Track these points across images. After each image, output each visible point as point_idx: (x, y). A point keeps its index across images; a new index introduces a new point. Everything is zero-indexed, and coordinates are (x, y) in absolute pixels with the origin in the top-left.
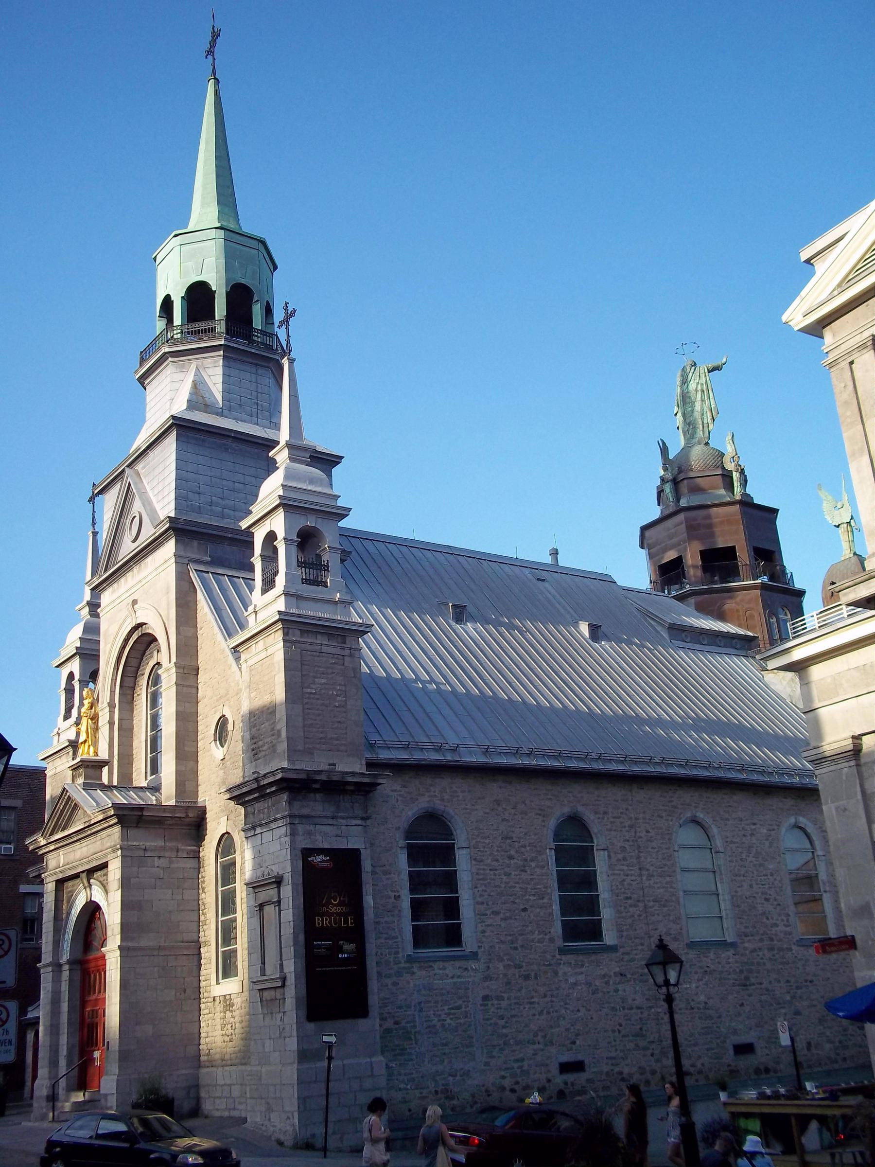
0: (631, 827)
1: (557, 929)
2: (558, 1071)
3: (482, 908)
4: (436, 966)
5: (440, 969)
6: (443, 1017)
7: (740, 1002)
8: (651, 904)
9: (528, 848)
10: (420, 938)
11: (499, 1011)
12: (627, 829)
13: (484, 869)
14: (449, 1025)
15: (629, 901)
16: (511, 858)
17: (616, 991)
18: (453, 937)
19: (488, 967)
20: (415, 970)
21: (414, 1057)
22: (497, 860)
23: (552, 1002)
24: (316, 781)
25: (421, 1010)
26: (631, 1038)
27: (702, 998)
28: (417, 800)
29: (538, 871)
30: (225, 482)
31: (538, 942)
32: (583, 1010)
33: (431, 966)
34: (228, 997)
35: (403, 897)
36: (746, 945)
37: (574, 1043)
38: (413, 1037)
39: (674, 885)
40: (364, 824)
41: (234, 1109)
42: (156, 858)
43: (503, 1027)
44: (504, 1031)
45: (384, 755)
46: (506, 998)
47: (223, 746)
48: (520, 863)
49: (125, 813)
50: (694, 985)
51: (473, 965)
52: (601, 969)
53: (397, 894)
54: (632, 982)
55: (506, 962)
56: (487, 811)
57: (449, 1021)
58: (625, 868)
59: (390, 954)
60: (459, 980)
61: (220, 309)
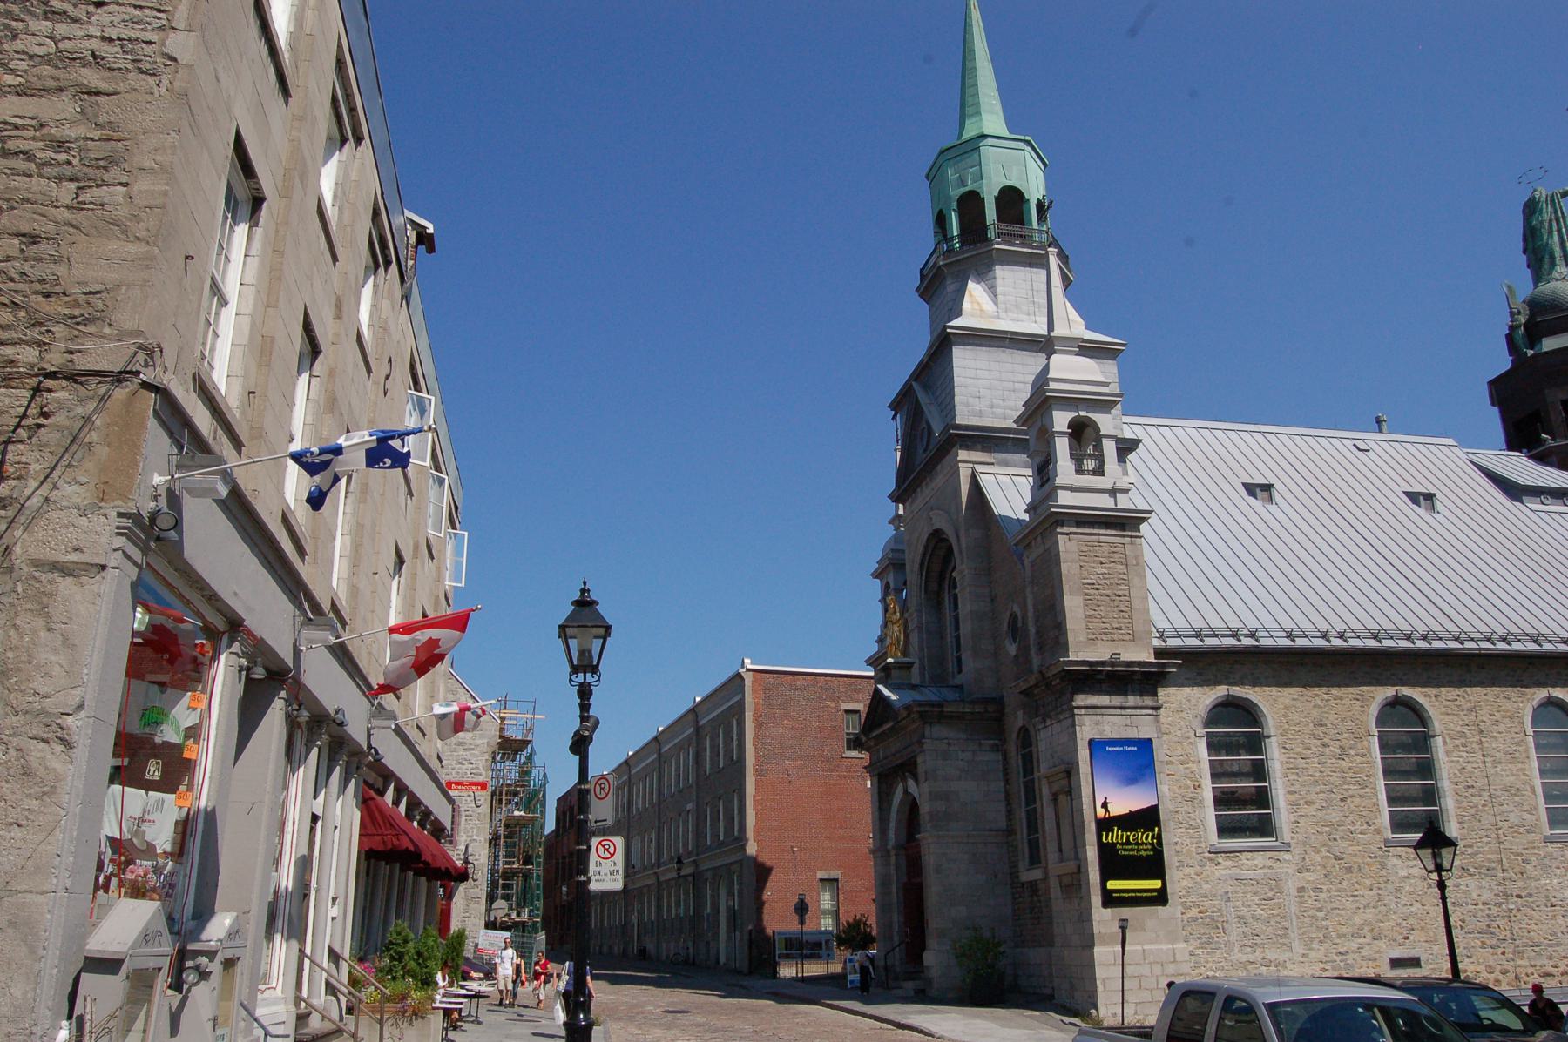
0: (1470, 711)
2: (1388, 967)
3: (1292, 797)
4: (1243, 856)
5: (1248, 859)
6: (1255, 907)
8: (1499, 793)
9: (1345, 735)
10: (1227, 829)
12: (1465, 712)
13: (1295, 758)
15: (1471, 790)
16: (1325, 745)
18: (1264, 827)
19: (1304, 858)
20: (1220, 861)
21: (1223, 946)
22: (1310, 749)
25: (1228, 900)
26: (1477, 935)
29: (1358, 759)
30: (1005, 384)
31: (1361, 833)
32: (1417, 906)
33: (1238, 856)
34: (1034, 883)
35: (1203, 786)
37: (1408, 938)
38: (1220, 926)
40: (1155, 713)
41: (1045, 987)
42: (960, 753)
43: (1324, 919)
44: (1324, 923)
45: (1173, 643)
46: (1325, 890)
47: (1015, 642)
48: (1338, 751)
51: (1287, 856)
53: (1196, 784)
54: (1477, 876)
55: (1325, 853)
56: (1296, 697)
57: (1260, 911)
58: (1465, 754)
59: (1192, 844)
61: (991, 214)
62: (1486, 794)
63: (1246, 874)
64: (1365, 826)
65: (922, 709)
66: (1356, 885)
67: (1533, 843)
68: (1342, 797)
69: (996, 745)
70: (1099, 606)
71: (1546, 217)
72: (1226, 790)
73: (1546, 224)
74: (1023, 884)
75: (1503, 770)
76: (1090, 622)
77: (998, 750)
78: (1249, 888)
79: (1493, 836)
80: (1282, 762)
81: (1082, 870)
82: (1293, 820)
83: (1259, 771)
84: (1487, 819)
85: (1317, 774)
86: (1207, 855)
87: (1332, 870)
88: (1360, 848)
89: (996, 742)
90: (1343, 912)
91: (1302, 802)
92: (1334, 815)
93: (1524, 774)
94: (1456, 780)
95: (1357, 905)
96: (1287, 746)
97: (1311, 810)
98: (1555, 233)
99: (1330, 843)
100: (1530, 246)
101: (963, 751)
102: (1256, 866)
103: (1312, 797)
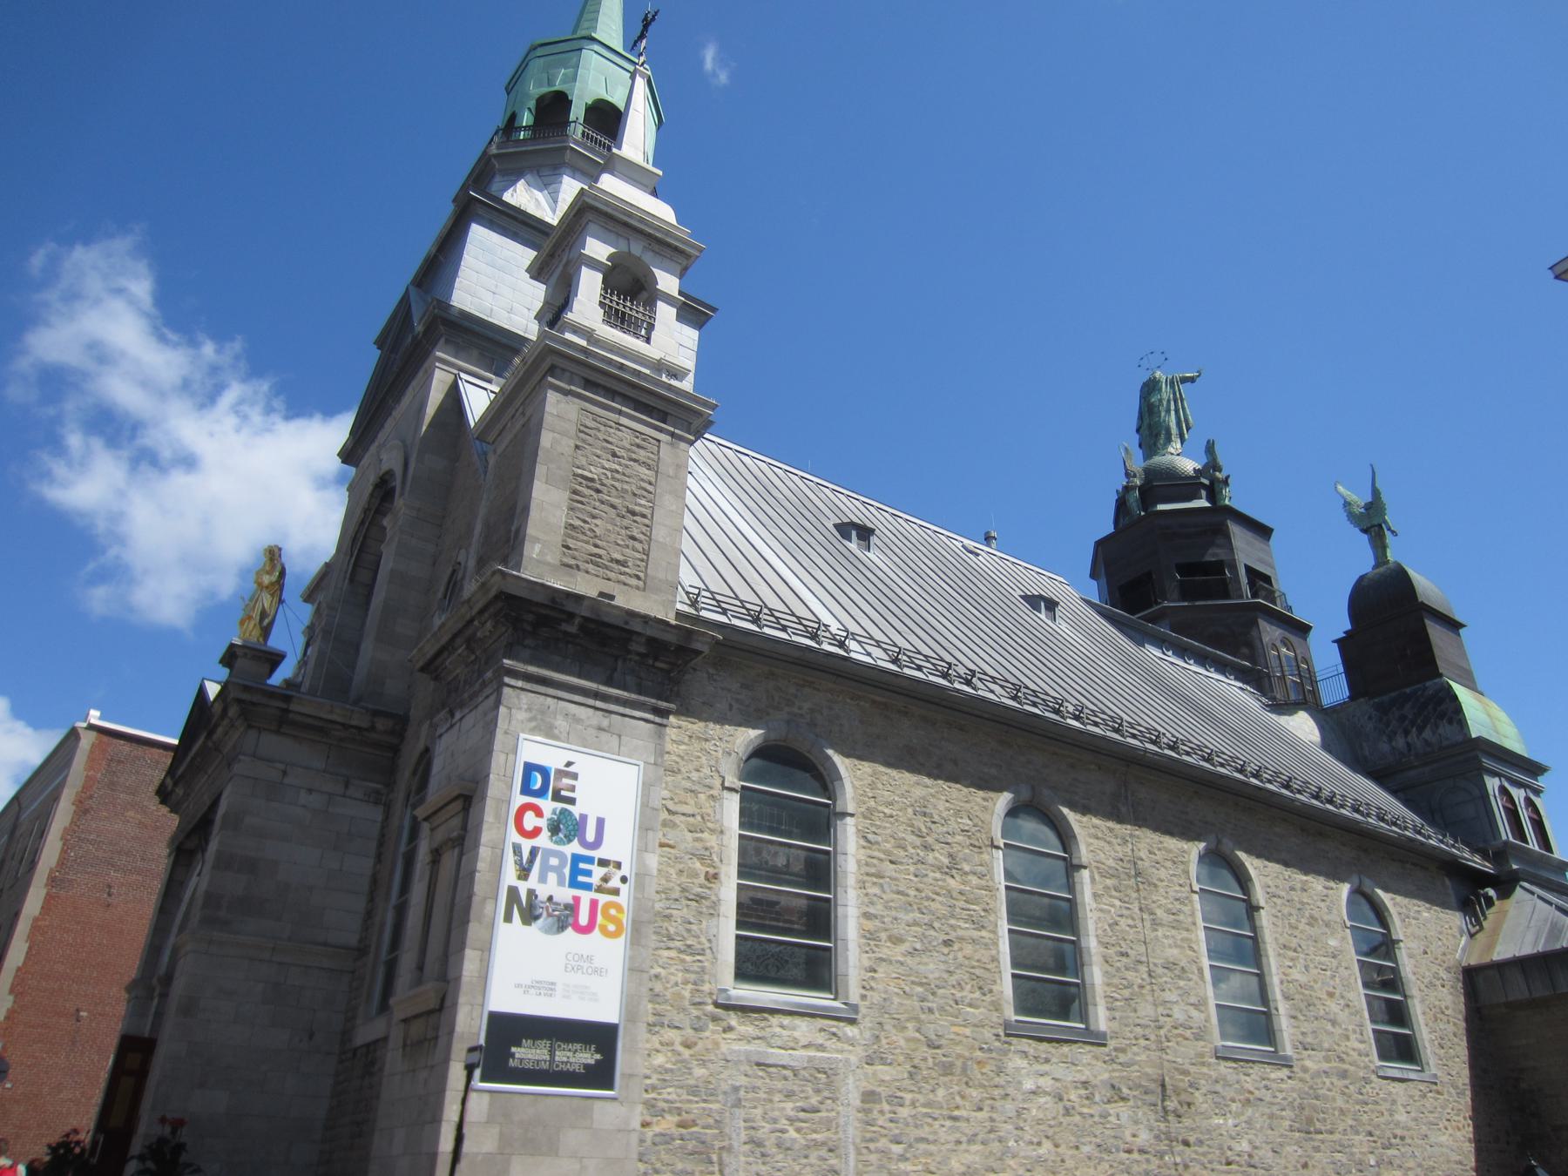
1: (1006, 987)
3: (870, 925)
7: (1303, 1160)
8: (1160, 971)
10: (751, 966)
11: (892, 1125)
13: (881, 860)
14: (794, 1140)
15: (1124, 959)
17: (1104, 1116)
20: (734, 1023)
22: (905, 849)
23: (992, 1120)
24: (571, 616)
25: (738, 1104)
27: (1244, 1146)
28: (768, 714)
29: (974, 880)
31: (970, 1005)
32: (1047, 1145)
33: (765, 1019)
35: (722, 877)
36: (1308, 1063)
38: (715, 1158)
39: (1193, 945)
43: (903, 1158)
46: (907, 1103)
48: (946, 861)
49: (256, 698)
50: (1230, 1122)
51: (850, 1031)
52: (1079, 1071)
53: (711, 871)
54: (1131, 1103)
55: (911, 1033)
57: (792, 1134)
58: (1117, 903)
59: (686, 982)
60: (820, 1054)
62: (1143, 969)
63: (778, 1055)
64: (977, 994)
65: (245, 696)
66: (958, 1098)
67: (1201, 1055)
68: (946, 937)
69: (377, 792)
70: (594, 517)
71: (1165, 396)
72: (759, 895)
73: (1165, 403)
74: (355, 1051)
75: (1166, 937)
76: (572, 538)
77: (376, 803)
78: (779, 1085)
79: (1153, 1037)
80: (858, 862)
81: (448, 1003)
82: (867, 963)
83: (820, 871)
84: (1146, 1010)
85: (912, 893)
86: (710, 1008)
87: (922, 1065)
88: (967, 1031)
89: (379, 786)
90: (932, 1148)
91: (883, 936)
92: (932, 967)
93: (1191, 948)
94: (1106, 940)
95: (958, 1135)
96: (870, 836)
97: (897, 952)
98: (1173, 413)
99: (923, 1017)
100: (1146, 422)
101: (310, 791)
102: (796, 1040)
103: (900, 930)
